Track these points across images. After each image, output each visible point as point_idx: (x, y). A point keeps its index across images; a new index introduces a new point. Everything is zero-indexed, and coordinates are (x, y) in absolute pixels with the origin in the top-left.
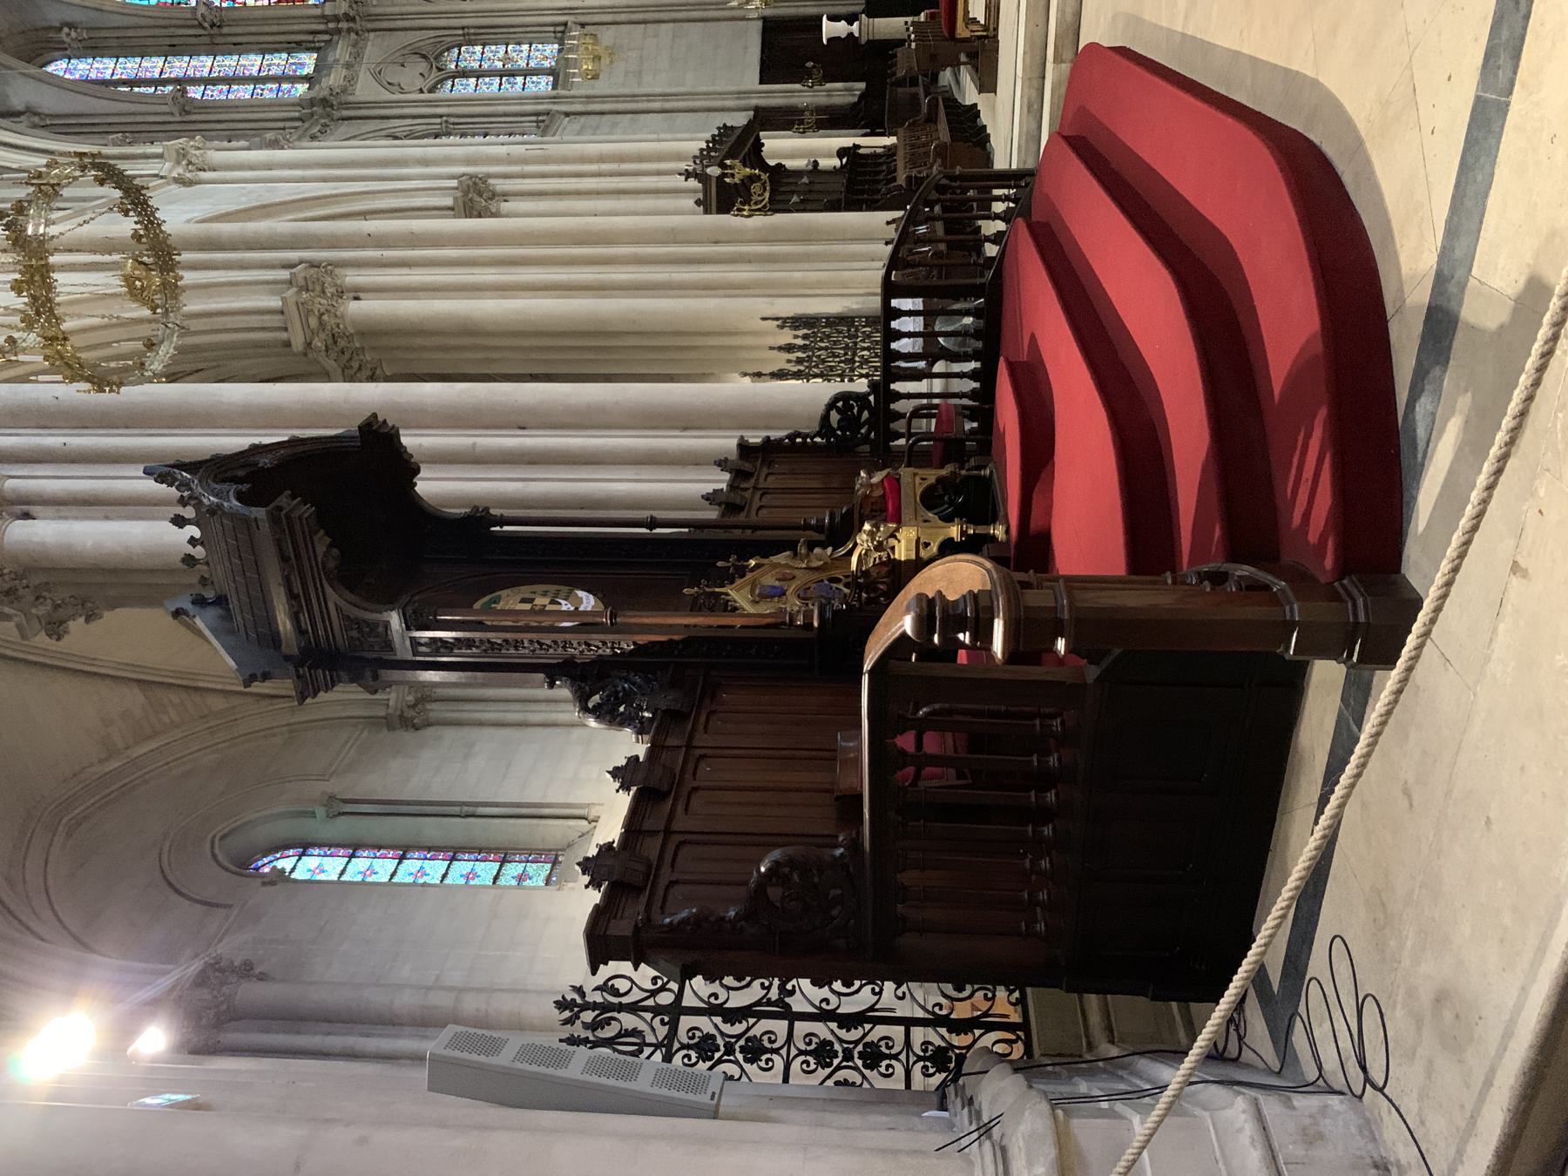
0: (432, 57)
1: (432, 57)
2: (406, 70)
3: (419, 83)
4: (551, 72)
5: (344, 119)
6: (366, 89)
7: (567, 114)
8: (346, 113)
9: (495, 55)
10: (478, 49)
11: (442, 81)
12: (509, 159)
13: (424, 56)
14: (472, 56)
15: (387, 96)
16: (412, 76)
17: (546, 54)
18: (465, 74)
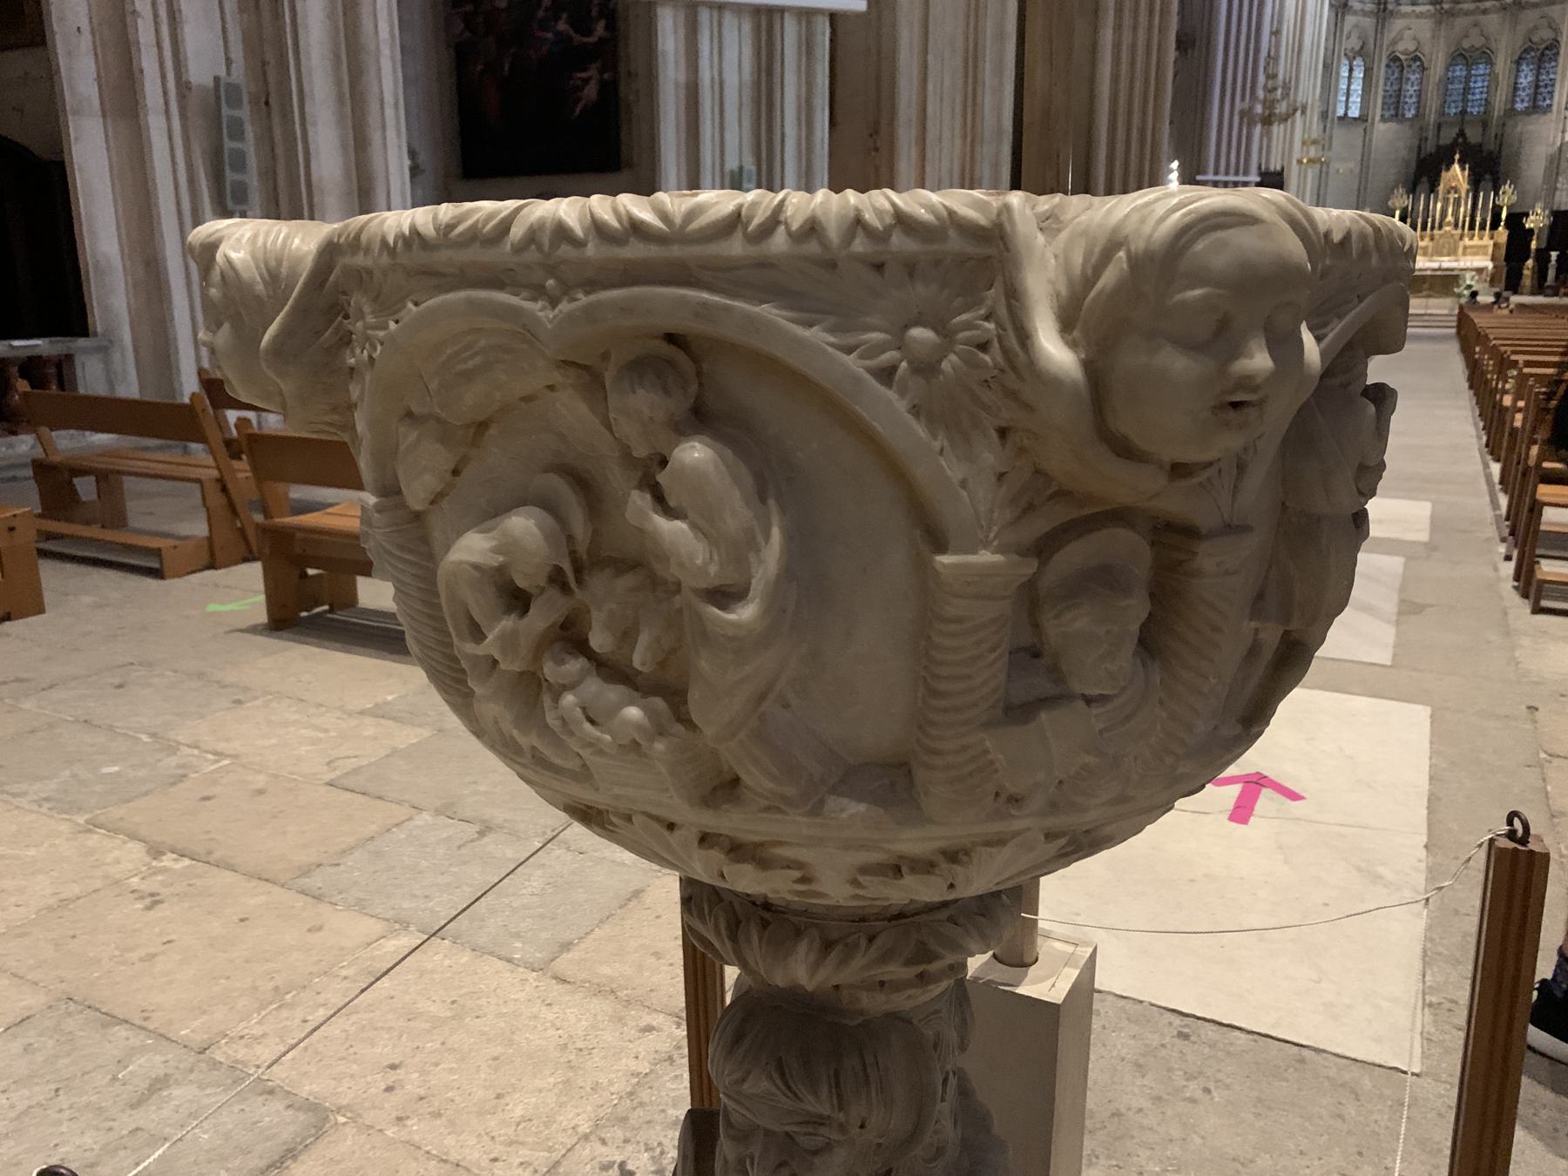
0: (1361, 52)
1: (1361, 52)
2: (1356, 41)
3: (1349, 47)
4: (1346, 114)
5: (1337, 15)
6: (1350, 20)
7: (1325, 127)
8: (1340, 15)
9: (1357, 86)
10: (1362, 75)
11: (1348, 59)
12: (1311, 123)
13: (1362, 48)
14: (1359, 74)
15: (1345, 33)
16: (1354, 43)
17: (1354, 112)
18: (1351, 70)
